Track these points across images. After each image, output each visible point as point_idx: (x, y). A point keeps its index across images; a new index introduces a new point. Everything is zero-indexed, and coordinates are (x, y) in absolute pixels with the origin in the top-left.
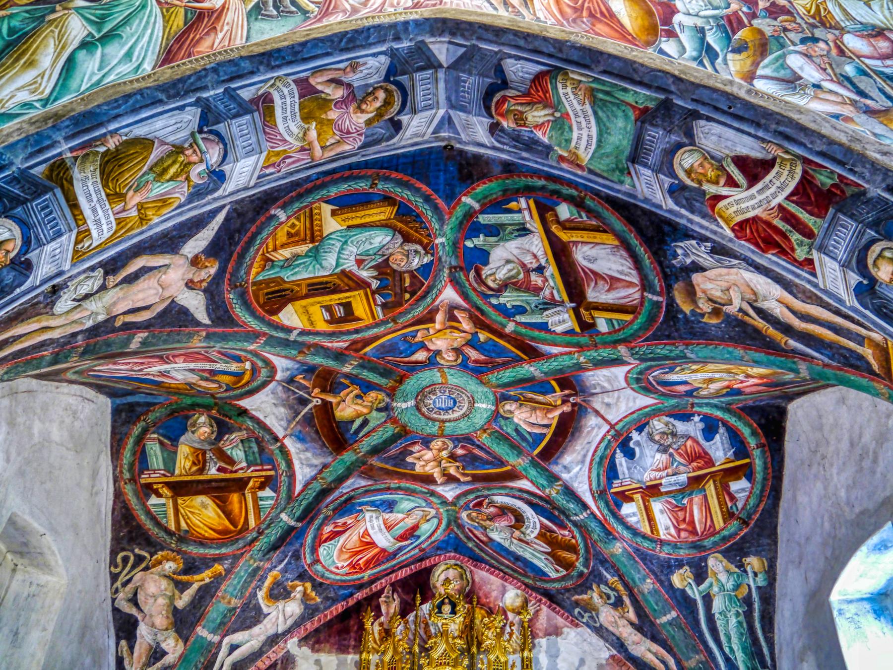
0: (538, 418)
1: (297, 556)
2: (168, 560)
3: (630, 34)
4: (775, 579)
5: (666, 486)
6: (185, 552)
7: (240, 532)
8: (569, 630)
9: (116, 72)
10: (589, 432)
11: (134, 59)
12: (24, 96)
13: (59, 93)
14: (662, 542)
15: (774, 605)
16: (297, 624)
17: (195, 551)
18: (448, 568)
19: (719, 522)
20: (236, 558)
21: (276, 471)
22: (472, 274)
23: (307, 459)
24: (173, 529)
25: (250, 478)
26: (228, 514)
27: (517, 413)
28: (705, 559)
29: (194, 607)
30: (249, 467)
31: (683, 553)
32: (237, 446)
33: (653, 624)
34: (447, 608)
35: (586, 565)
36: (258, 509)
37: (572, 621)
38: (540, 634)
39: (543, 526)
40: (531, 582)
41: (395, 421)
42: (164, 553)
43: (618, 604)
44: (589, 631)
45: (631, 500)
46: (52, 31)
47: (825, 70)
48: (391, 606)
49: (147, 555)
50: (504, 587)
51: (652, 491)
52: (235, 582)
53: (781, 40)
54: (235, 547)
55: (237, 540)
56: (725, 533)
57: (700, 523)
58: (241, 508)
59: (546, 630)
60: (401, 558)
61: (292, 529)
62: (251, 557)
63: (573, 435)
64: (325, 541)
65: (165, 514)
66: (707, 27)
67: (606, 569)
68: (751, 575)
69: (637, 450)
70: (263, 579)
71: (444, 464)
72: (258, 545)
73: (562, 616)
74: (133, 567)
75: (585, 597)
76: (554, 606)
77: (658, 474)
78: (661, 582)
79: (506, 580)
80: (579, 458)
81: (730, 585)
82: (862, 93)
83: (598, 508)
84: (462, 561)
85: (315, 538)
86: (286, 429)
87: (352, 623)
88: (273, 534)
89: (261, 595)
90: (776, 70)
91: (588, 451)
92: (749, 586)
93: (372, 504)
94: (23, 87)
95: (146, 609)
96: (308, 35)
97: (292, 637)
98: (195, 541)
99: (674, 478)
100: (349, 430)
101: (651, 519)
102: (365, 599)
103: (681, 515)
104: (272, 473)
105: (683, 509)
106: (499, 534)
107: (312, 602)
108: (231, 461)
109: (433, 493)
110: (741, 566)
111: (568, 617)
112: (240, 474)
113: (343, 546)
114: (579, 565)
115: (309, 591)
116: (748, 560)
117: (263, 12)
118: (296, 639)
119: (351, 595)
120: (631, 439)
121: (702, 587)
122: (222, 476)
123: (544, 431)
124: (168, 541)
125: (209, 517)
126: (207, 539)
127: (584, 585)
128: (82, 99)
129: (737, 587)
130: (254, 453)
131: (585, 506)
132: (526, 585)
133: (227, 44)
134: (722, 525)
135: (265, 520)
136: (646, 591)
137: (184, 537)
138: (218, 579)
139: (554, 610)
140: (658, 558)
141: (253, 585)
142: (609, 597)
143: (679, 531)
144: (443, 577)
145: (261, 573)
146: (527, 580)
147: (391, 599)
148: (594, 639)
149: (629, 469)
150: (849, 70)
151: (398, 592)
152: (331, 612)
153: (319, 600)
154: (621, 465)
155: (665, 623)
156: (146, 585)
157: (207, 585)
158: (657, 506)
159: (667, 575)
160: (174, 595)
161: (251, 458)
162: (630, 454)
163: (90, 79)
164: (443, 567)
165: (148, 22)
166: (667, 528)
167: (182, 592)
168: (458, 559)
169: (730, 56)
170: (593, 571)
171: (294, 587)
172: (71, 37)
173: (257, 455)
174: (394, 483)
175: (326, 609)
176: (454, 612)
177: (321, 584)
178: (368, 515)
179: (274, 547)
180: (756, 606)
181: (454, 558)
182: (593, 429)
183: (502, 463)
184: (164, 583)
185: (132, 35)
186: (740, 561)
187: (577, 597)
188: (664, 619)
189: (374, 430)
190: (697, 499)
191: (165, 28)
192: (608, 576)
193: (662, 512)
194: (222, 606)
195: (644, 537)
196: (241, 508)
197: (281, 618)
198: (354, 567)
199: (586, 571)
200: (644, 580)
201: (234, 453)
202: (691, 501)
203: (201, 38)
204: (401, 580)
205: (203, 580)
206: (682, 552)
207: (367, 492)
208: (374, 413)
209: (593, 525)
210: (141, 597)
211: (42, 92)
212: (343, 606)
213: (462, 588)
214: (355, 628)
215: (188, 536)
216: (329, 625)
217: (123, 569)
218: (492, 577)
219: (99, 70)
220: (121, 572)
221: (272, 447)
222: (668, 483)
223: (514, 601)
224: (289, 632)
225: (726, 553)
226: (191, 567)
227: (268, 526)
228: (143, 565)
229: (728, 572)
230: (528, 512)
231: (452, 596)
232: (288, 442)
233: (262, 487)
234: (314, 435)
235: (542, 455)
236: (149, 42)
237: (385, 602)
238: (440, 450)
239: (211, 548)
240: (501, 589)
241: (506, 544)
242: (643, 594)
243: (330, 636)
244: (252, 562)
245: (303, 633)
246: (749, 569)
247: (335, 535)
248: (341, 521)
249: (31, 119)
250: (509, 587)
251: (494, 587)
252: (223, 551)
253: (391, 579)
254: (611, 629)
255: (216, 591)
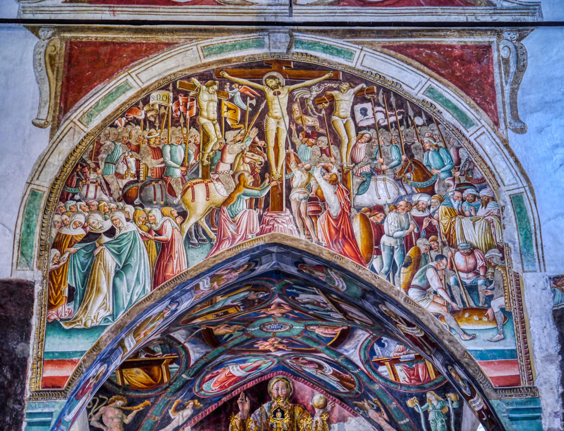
0: (330, 331)
1: (190, 390)
2: (118, 400)
3: (360, 254)
4: (463, 405)
5: (403, 359)
6: (128, 395)
7: (159, 384)
8: (351, 418)
9: (136, 293)
10: (358, 337)
11: (141, 282)
12: (103, 313)
13: (116, 310)
14: (401, 385)
15: (462, 417)
16: (190, 419)
17: (134, 394)
18: (278, 381)
19: (433, 376)
20: (157, 397)
21: (179, 356)
22: (290, 297)
23: (197, 350)
24: (120, 384)
25: (164, 360)
26: (152, 376)
27: (317, 330)
28: (425, 394)
29: (135, 422)
30: (163, 354)
31: (413, 390)
32: (157, 346)
33: (396, 423)
34: (279, 414)
35: (360, 389)
36: (169, 373)
37: (354, 413)
38: (334, 421)
39: (333, 370)
40: (329, 391)
41: (248, 334)
42: (116, 397)
43: (378, 410)
44: (363, 418)
45: (384, 365)
46: (100, 264)
47: (441, 280)
48: (245, 406)
49: (106, 398)
50: (313, 392)
51: (396, 361)
52: (158, 408)
53: (427, 258)
54: (156, 391)
55: (157, 388)
56: (436, 381)
57: (422, 376)
58: (159, 373)
59: (338, 419)
60: (249, 378)
61: (188, 381)
62: (166, 396)
63: (349, 338)
64: (207, 381)
65: (116, 377)
66: (396, 247)
67: (371, 395)
68: (450, 402)
69: (386, 344)
70: (171, 405)
71: (275, 345)
72: (169, 390)
73: (347, 410)
74: (99, 404)
75: (360, 403)
76: (343, 403)
77: (398, 354)
78: (401, 404)
79: (314, 388)
80: (353, 346)
81: (438, 407)
82: (453, 299)
83: (365, 368)
84: (287, 376)
85: (201, 381)
86: (185, 339)
87: (222, 416)
88: (178, 384)
89: (170, 411)
90: (420, 281)
91: (358, 344)
92: (449, 408)
93: (234, 362)
94: (100, 307)
95: (108, 425)
96: (214, 261)
97: (187, 426)
98: (133, 390)
99: (408, 355)
100: (222, 339)
101: (395, 374)
102: (229, 401)
103: (411, 372)
104: (177, 357)
105: (413, 369)
106: (309, 369)
107: (198, 408)
108: (154, 352)
109: (269, 355)
110: (445, 397)
111: (351, 410)
112: (159, 358)
113: (217, 381)
114: (356, 389)
115: (196, 403)
116: (449, 395)
117: (191, 242)
118: (189, 427)
119: (220, 399)
120: (382, 339)
121: (423, 407)
122: (148, 359)
123: (333, 336)
124: (118, 390)
125: (141, 378)
126: (140, 388)
127: (360, 399)
128: (127, 314)
129: (442, 408)
130: (166, 348)
131: (358, 367)
132: (326, 391)
133: (179, 269)
134: (435, 377)
135: (173, 377)
136: (392, 408)
137: (126, 388)
138: (147, 408)
139: (343, 406)
140: (399, 392)
141: (167, 408)
142: (373, 406)
143: (410, 380)
144: (275, 386)
145: (171, 402)
146: (327, 390)
147: (244, 401)
148: (366, 423)
149: (382, 351)
150: (452, 280)
151: (248, 396)
152: (209, 410)
153: (201, 405)
154: (377, 350)
155: (402, 425)
156: (107, 413)
157: (141, 411)
158: (398, 368)
159: (404, 400)
160: (123, 417)
161: (165, 350)
162: (382, 345)
163: (126, 299)
164: (275, 380)
165: (140, 254)
166: (404, 378)
167: (127, 415)
168: (284, 375)
169: (403, 268)
170: (364, 393)
171: (188, 404)
172: (110, 268)
173: (169, 350)
174: (246, 354)
175: (205, 409)
176: (283, 417)
177: (203, 399)
178: (231, 367)
179: (179, 390)
180: (452, 417)
181: (282, 374)
182: (360, 335)
183: (309, 347)
184: (117, 412)
185: (136, 265)
186: (445, 395)
187: (355, 402)
188: (402, 422)
189: (236, 338)
190: (420, 365)
191: (149, 257)
192: (372, 397)
193: (401, 370)
194: (151, 421)
195: (391, 382)
196: (159, 373)
197: (181, 418)
198: (222, 387)
199: (360, 392)
200: (392, 403)
201: (155, 348)
202: (417, 366)
203: (167, 264)
204: (250, 388)
205: (139, 409)
206: (412, 390)
207: (231, 359)
208: (236, 332)
209: (362, 376)
210: (104, 419)
211: (109, 309)
212: (215, 406)
213: (287, 393)
214: (224, 420)
215: (130, 387)
216: (208, 418)
217: (93, 406)
218: (306, 386)
219: (128, 292)
220: (92, 408)
221: (178, 347)
222: (403, 358)
223: (319, 402)
224: (186, 423)
225: (437, 391)
226: (132, 402)
227: (175, 381)
228: (104, 403)
229: (438, 401)
230: (326, 365)
231: (282, 407)
232: (187, 345)
233: (171, 363)
234: (201, 341)
235: (331, 345)
236: (145, 269)
237: (241, 402)
238: (273, 341)
239: (142, 392)
240: (311, 393)
241: (314, 374)
242: (391, 409)
243: (209, 425)
244: (166, 398)
245: (193, 424)
246: (449, 399)
247: (211, 378)
248: (215, 372)
249: (111, 329)
250: (316, 392)
251: (307, 393)
252: (150, 394)
253: (243, 388)
254: (375, 420)
255: (147, 414)
